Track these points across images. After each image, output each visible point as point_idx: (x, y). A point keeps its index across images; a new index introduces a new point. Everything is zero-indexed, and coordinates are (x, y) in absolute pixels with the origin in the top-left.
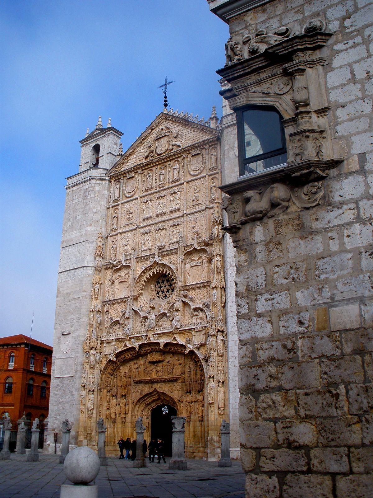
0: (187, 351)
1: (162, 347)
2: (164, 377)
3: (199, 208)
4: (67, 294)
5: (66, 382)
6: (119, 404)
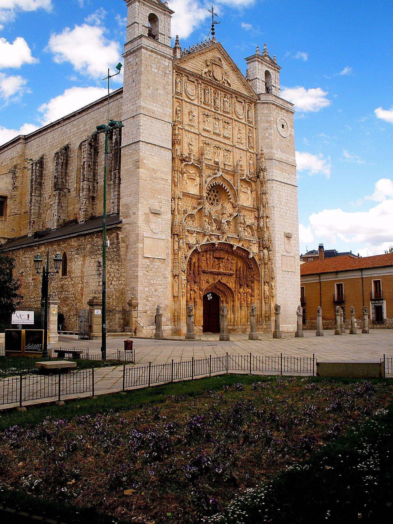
0: (251, 256)
1: (235, 248)
2: (228, 272)
3: (241, 147)
4: (154, 169)
5: (157, 264)
6: (194, 291)
